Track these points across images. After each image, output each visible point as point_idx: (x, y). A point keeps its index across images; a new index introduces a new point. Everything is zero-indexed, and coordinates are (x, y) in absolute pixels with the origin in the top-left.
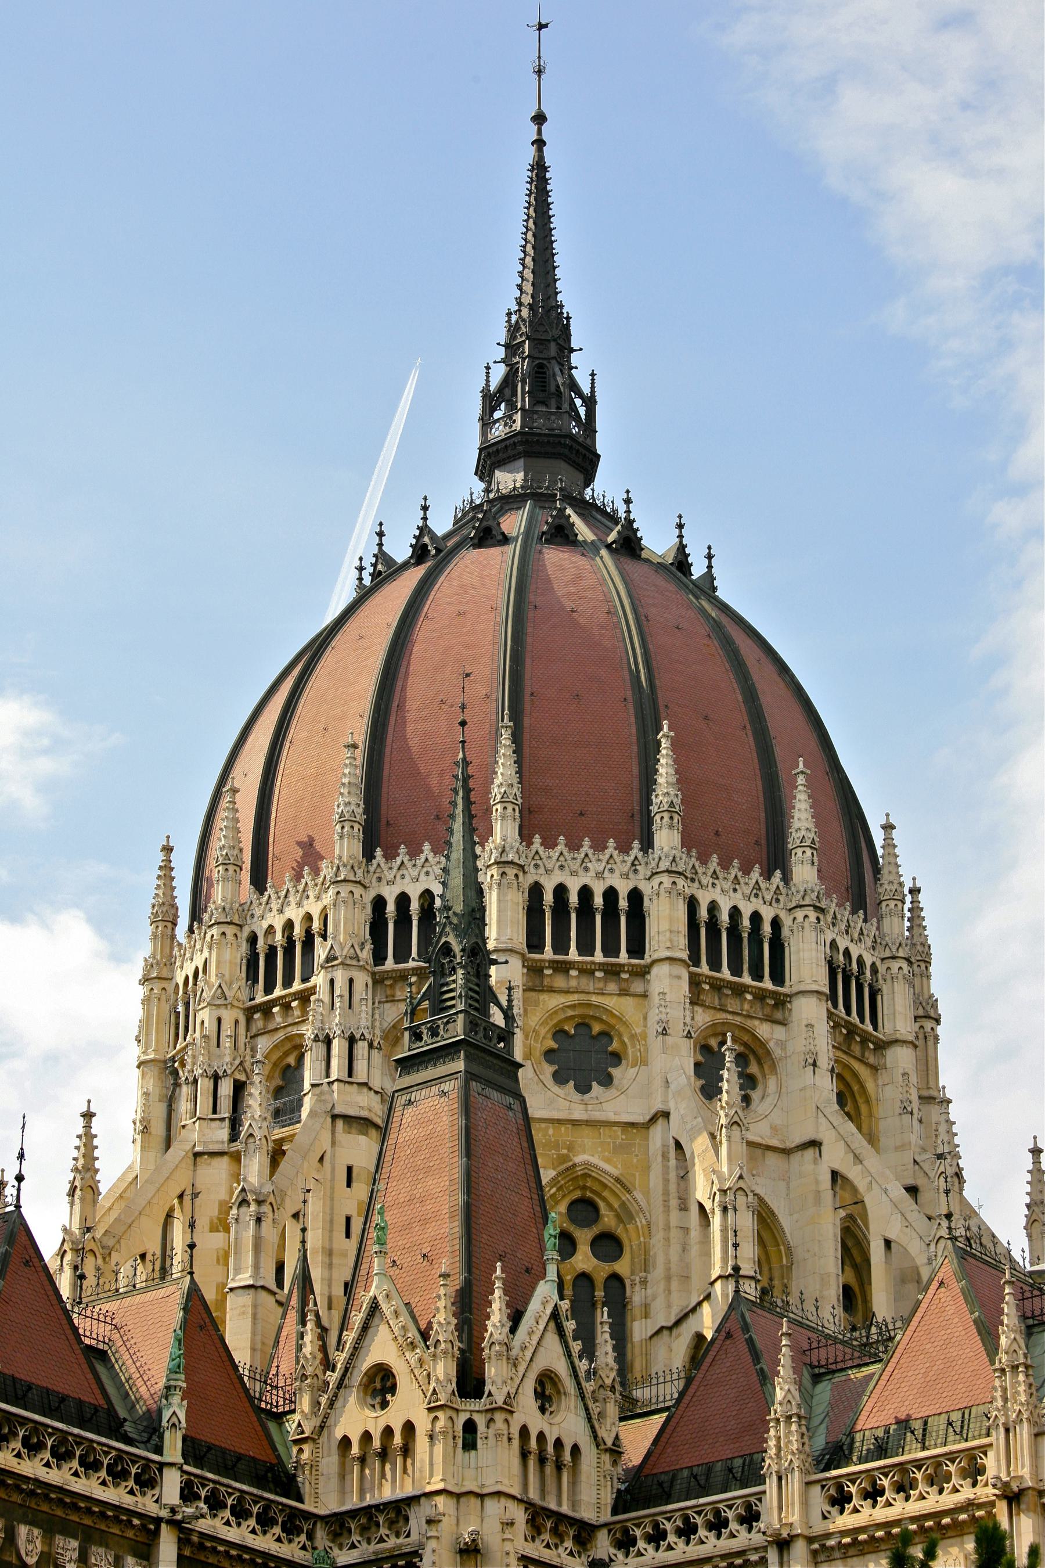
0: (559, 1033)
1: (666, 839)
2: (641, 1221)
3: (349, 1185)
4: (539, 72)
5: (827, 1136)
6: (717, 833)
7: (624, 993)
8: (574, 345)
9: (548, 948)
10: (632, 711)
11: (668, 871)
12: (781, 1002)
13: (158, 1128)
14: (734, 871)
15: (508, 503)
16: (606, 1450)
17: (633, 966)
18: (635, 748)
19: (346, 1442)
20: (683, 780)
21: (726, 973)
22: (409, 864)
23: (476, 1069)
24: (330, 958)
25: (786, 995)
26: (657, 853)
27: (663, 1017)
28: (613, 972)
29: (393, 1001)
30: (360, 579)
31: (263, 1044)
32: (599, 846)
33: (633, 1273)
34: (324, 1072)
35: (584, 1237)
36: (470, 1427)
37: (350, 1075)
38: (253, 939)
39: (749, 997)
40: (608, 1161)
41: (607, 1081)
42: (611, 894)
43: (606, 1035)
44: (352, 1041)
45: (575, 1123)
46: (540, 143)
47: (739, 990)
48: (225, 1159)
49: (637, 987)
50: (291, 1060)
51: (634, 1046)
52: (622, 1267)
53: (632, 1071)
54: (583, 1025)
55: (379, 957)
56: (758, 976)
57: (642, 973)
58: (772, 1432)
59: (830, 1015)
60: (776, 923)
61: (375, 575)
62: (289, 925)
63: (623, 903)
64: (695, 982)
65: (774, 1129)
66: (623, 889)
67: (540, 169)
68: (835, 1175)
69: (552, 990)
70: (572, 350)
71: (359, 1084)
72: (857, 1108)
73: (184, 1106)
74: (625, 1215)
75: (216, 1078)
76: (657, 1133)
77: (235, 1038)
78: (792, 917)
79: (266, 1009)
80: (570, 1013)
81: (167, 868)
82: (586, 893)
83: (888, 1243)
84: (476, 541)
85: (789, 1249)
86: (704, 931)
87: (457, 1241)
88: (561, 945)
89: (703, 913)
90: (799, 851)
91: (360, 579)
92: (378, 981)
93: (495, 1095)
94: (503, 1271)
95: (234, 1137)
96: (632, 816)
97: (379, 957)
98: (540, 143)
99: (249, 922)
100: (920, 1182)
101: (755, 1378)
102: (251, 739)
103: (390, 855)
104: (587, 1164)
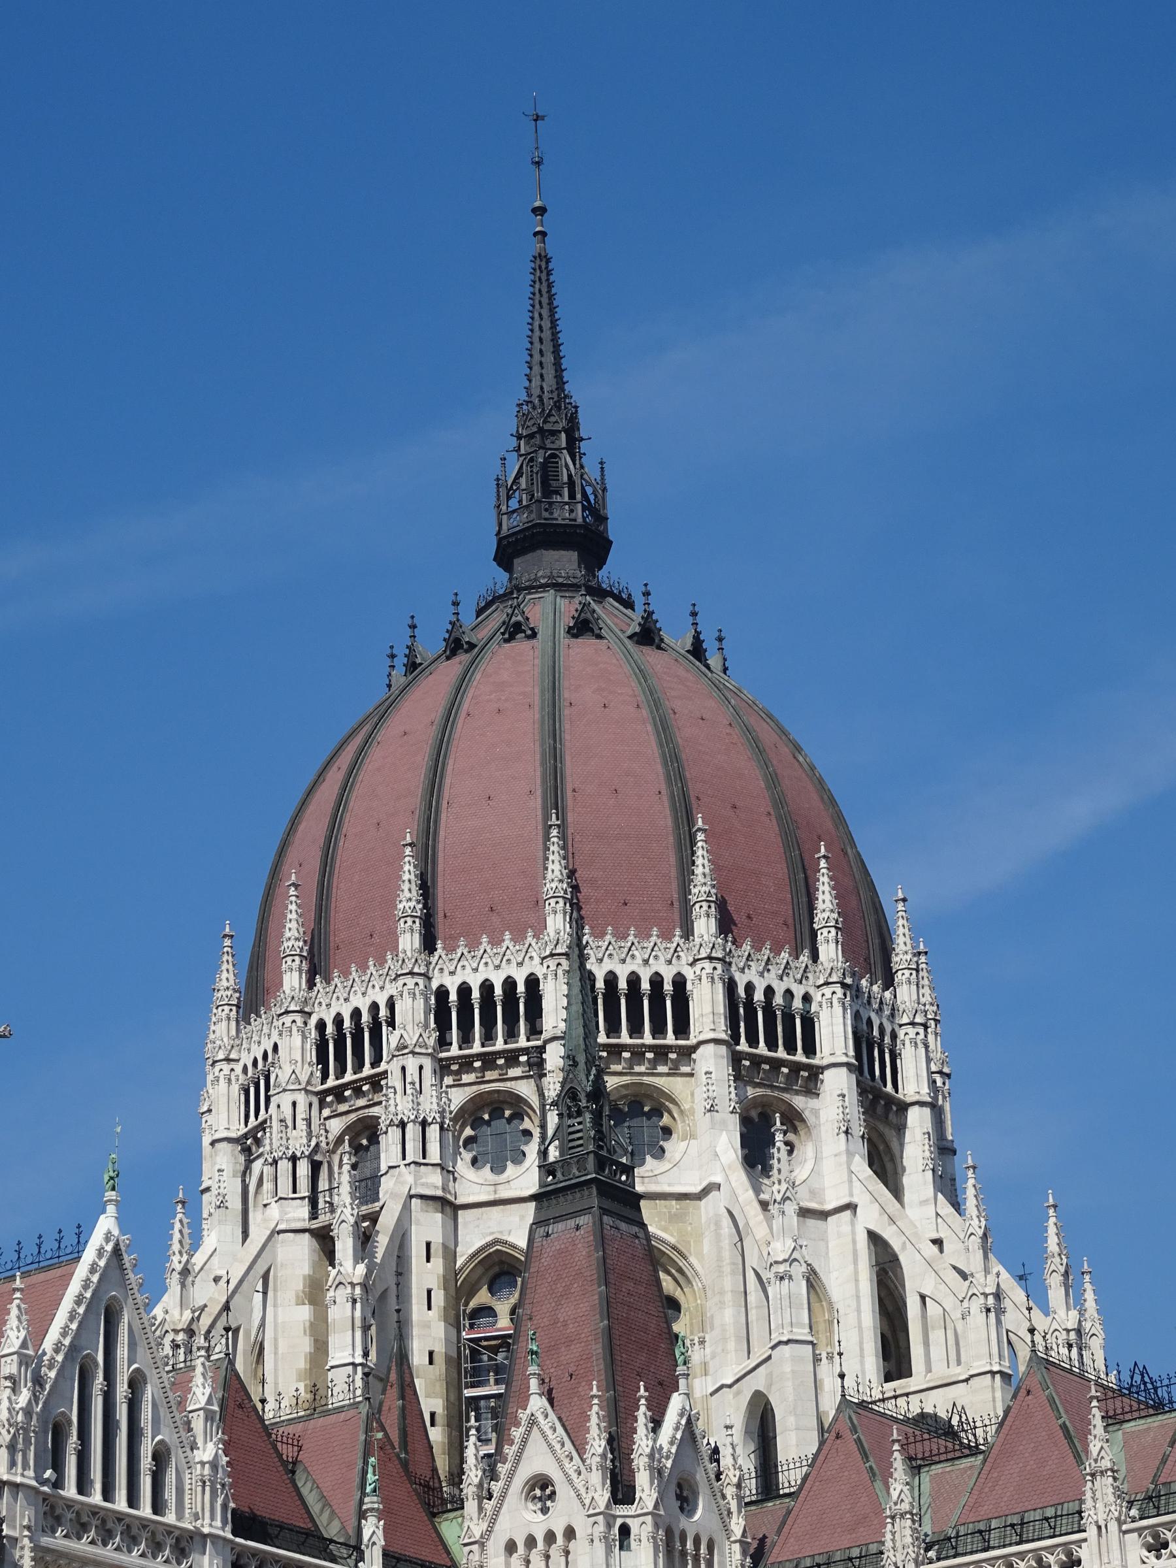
2: (697, 1285)
3: (428, 1260)
5: (860, 1197)
6: (749, 917)
10: (666, 804)
11: (710, 958)
12: (815, 1073)
14: (766, 952)
15: (530, 593)
16: (735, 1542)
17: (680, 1047)
18: (671, 839)
21: (762, 1049)
22: (469, 956)
23: (608, 1204)
24: (401, 1047)
25: (818, 1067)
26: (698, 940)
27: (710, 1094)
31: (336, 1126)
32: (644, 935)
33: (692, 1333)
34: (400, 1155)
36: (625, 1531)
37: (424, 1157)
38: (321, 1026)
40: (665, 1230)
41: (660, 1153)
42: (657, 981)
44: (424, 1124)
47: (777, 1064)
51: (684, 1121)
53: (684, 1144)
55: (443, 1043)
56: (791, 1048)
57: (687, 1053)
58: (889, 1526)
59: (858, 1083)
60: (807, 998)
61: (412, 666)
62: (356, 1013)
63: (668, 987)
64: (736, 1059)
66: (668, 974)
70: (582, 439)
71: (433, 1165)
72: (883, 1167)
75: (294, 1159)
76: (713, 1205)
77: (309, 1122)
78: (820, 993)
79: (338, 1093)
80: (625, 1092)
82: (634, 980)
83: (923, 1298)
84: (507, 636)
85: (830, 1304)
87: (601, 1361)
89: (741, 992)
90: (825, 931)
92: (443, 1067)
93: (623, 1226)
94: (646, 1390)
95: (314, 1215)
96: (672, 904)
97: (443, 1043)
99: (317, 1009)
100: (943, 1234)
101: (866, 1476)
102: (301, 828)
103: (450, 949)
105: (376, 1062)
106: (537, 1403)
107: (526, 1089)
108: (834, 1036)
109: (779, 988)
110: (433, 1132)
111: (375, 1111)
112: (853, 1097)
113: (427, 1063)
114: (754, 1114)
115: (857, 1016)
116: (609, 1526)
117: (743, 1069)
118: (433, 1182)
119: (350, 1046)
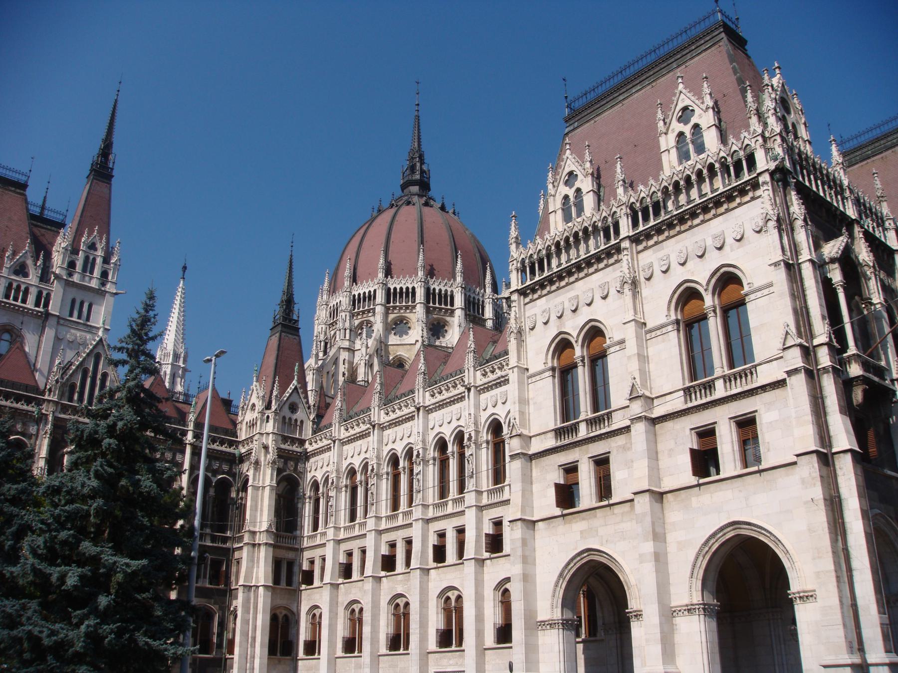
12: (453, 311)
21: (437, 305)
28: (407, 307)
36: (268, 417)
41: (407, 334)
42: (407, 288)
47: (441, 309)
56: (446, 304)
57: (414, 307)
82: (401, 289)
86: (429, 294)
108: (459, 301)
109: (443, 289)
110: (348, 331)
112: (463, 317)
113: (348, 314)
115: (465, 295)
116: (263, 416)
117: (428, 311)
118: (346, 344)
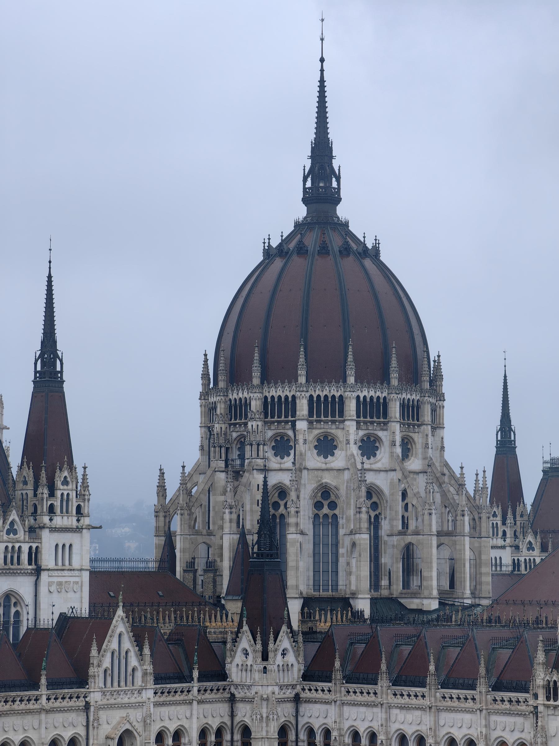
0: (318, 440)
1: (351, 380)
4: (322, 40)
7: (337, 428)
8: (333, 155)
9: (315, 416)
12: (385, 424)
13: (206, 448)
19: (238, 665)
20: (355, 360)
28: (333, 422)
29: (270, 429)
30: (264, 247)
31: (235, 435)
35: (326, 503)
36: (265, 668)
39: (375, 424)
41: (333, 454)
43: (333, 440)
44: (258, 445)
45: (323, 470)
46: (322, 71)
48: (224, 473)
49: (341, 426)
50: (243, 440)
52: (337, 512)
53: (340, 452)
54: (326, 437)
55: (266, 417)
65: (383, 464)
66: (337, 395)
67: (322, 81)
68: (399, 480)
69: (316, 428)
73: (212, 454)
74: (337, 497)
75: (221, 447)
79: (235, 424)
81: (206, 361)
83: (413, 505)
88: (319, 415)
91: (264, 247)
92: (265, 423)
97: (266, 417)
98: (322, 71)
104: (326, 483)
105: (246, 418)
106: (246, 628)
107: (290, 433)
111: (245, 433)
114: (365, 439)
119: (238, 410)
